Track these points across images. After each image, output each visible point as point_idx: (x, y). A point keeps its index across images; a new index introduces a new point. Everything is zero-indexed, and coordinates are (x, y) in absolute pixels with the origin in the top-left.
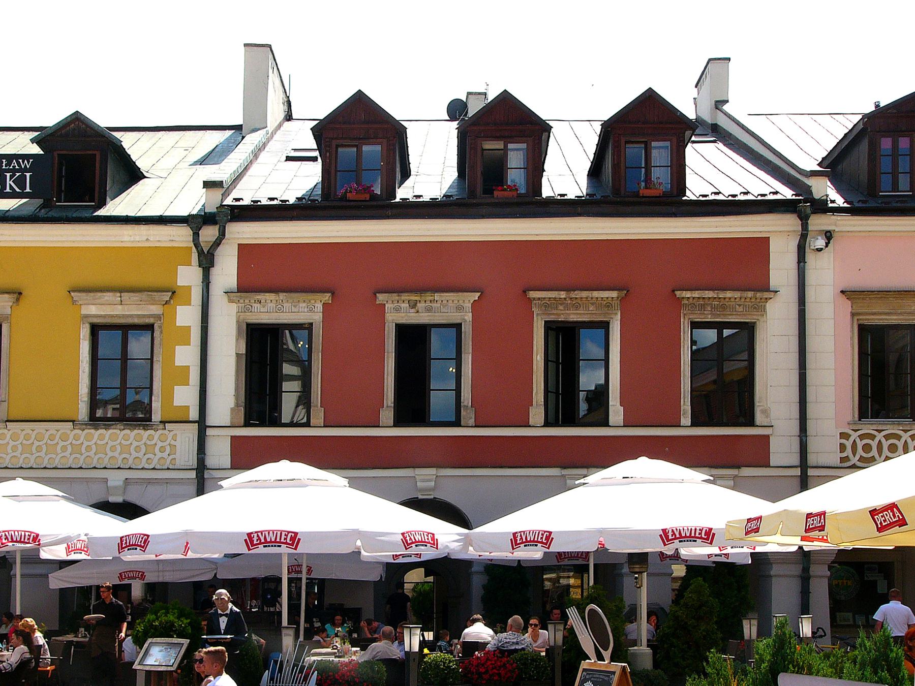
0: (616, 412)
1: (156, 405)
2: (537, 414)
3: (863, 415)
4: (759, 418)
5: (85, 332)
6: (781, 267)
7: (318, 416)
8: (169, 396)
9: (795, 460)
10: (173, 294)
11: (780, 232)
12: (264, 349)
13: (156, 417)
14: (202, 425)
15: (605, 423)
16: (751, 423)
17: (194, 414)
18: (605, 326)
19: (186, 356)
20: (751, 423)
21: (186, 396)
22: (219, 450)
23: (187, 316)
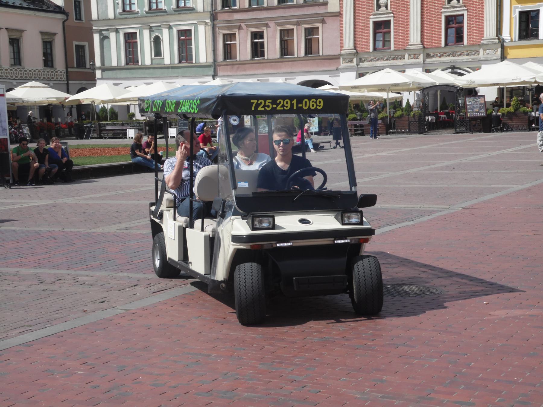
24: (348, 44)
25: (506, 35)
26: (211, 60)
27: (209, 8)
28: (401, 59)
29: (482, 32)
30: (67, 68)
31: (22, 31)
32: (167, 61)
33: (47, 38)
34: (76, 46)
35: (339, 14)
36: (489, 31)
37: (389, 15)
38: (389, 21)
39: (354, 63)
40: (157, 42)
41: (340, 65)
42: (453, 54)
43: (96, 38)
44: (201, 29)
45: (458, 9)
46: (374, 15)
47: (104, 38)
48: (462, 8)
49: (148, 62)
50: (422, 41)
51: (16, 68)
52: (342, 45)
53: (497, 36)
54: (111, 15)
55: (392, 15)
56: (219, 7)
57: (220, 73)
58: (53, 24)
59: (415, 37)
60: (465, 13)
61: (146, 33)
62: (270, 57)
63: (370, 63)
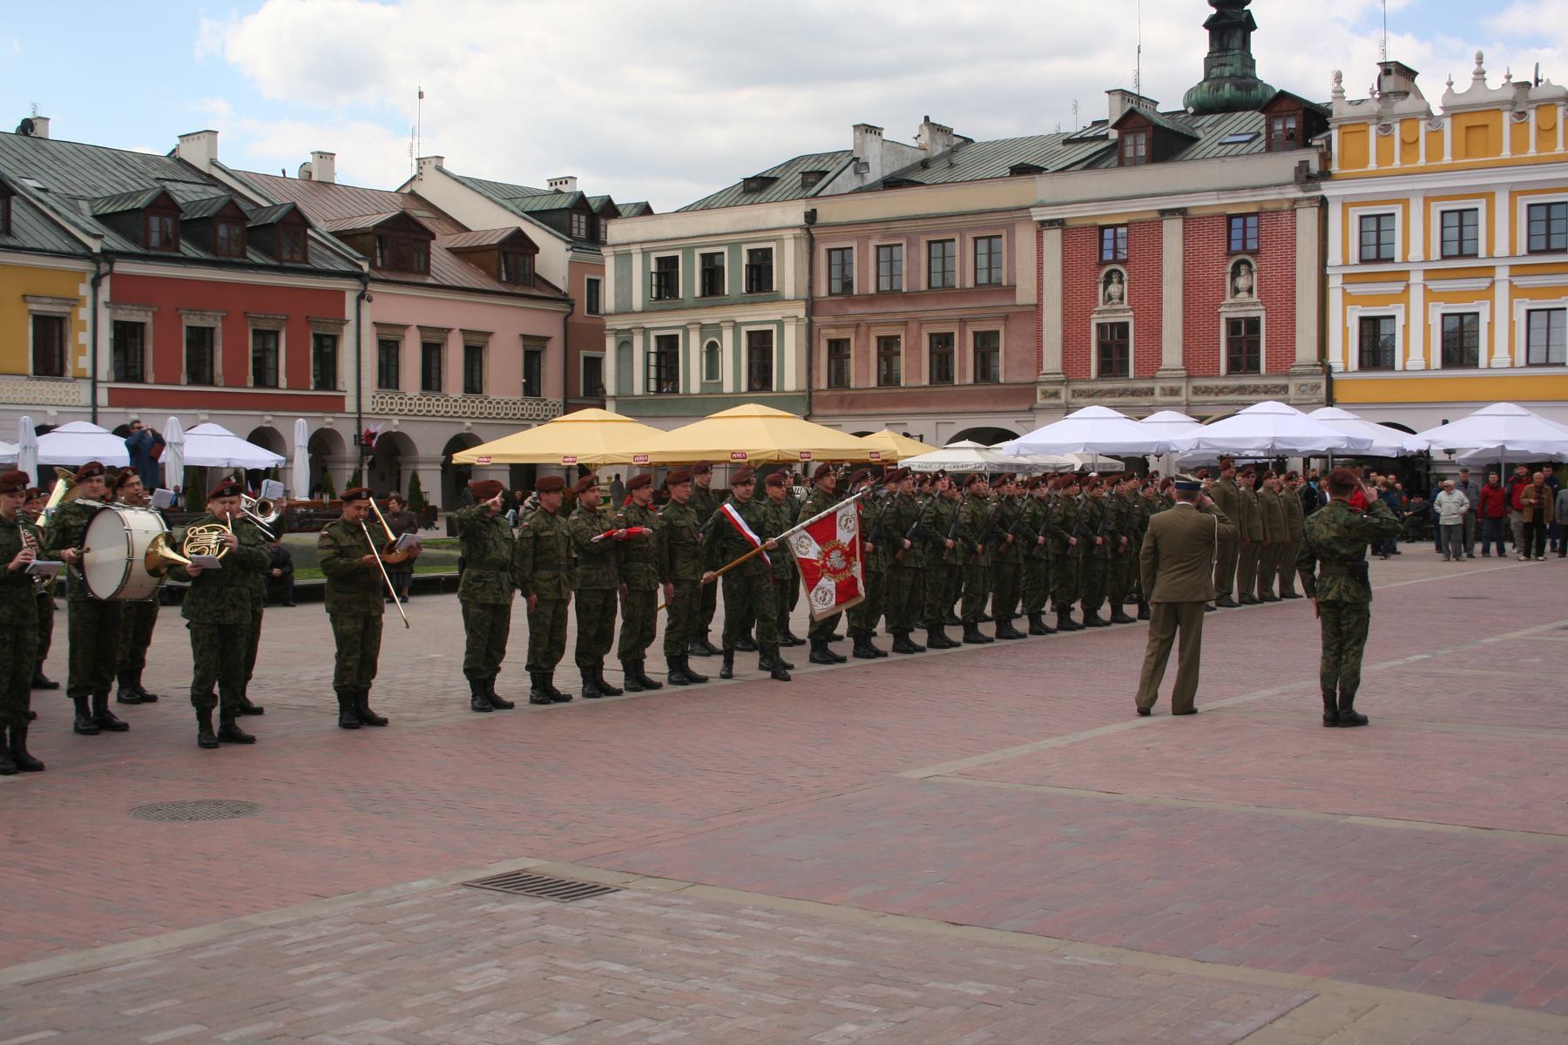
0: (283, 381)
1: (69, 366)
2: (250, 383)
3: (380, 386)
4: (340, 386)
5: (31, 320)
6: (350, 313)
7: (150, 377)
8: (76, 362)
9: (89, 401)
10: (75, 302)
11: (350, 288)
12: (126, 337)
13: (70, 373)
14: (95, 382)
15: (276, 386)
16: (334, 389)
17: (89, 373)
18: (276, 333)
19: (85, 338)
20: (334, 389)
21: (85, 362)
22: (103, 397)
23: (85, 314)
24: (1052, 360)
25: (1335, 358)
26: (804, 386)
27: (804, 294)
28: (1146, 394)
30: (566, 399)
31: (489, 334)
32: (728, 387)
33: (532, 345)
34: (586, 359)
35: (1038, 307)
36: (1306, 350)
38: (1126, 325)
40: (712, 351)
43: (611, 344)
44: (790, 332)
46: (1100, 312)
47: (625, 345)
49: (695, 388)
50: (1184, 363)
51: (473, 397)
52: (1040, 366)
54: (637, 302)
56: (822, 291)
57: (816, 411)
58: (545, 322)
59: (1172, 354)
61: (695, 338)
62: (912, 383)
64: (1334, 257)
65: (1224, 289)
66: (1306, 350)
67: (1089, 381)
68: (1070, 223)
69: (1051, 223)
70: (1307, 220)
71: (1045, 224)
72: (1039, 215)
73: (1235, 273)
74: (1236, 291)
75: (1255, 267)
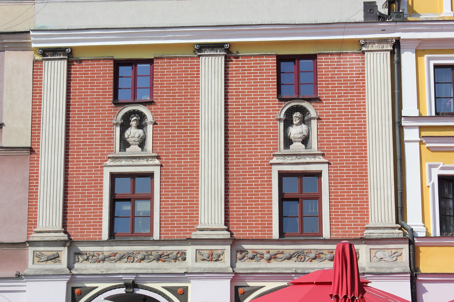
24: (49, 218)
28: (176, 259)
29: (363, 211)
36: (381, 212)
37: (150, 163)
39: (63, 264)
41: (26, 266)
42: (299, 256)
45: (308, 160)
48: (317, 160)
52: (32, 221)
53: (397, 222)
55: (157, 162)
59: (210, 213)
60: (324, 169)
63: (101, 265)
64: (409, 108)
65: (276, 139)
66: (381, 212)
67: (100, 243)
68: (77, 55)
69: (55, 51)
70: (377, 64)
71: (45, 52)
72: (38, 42)
73: (288, 122)
74: (288, 142)
75: (313, 113)
